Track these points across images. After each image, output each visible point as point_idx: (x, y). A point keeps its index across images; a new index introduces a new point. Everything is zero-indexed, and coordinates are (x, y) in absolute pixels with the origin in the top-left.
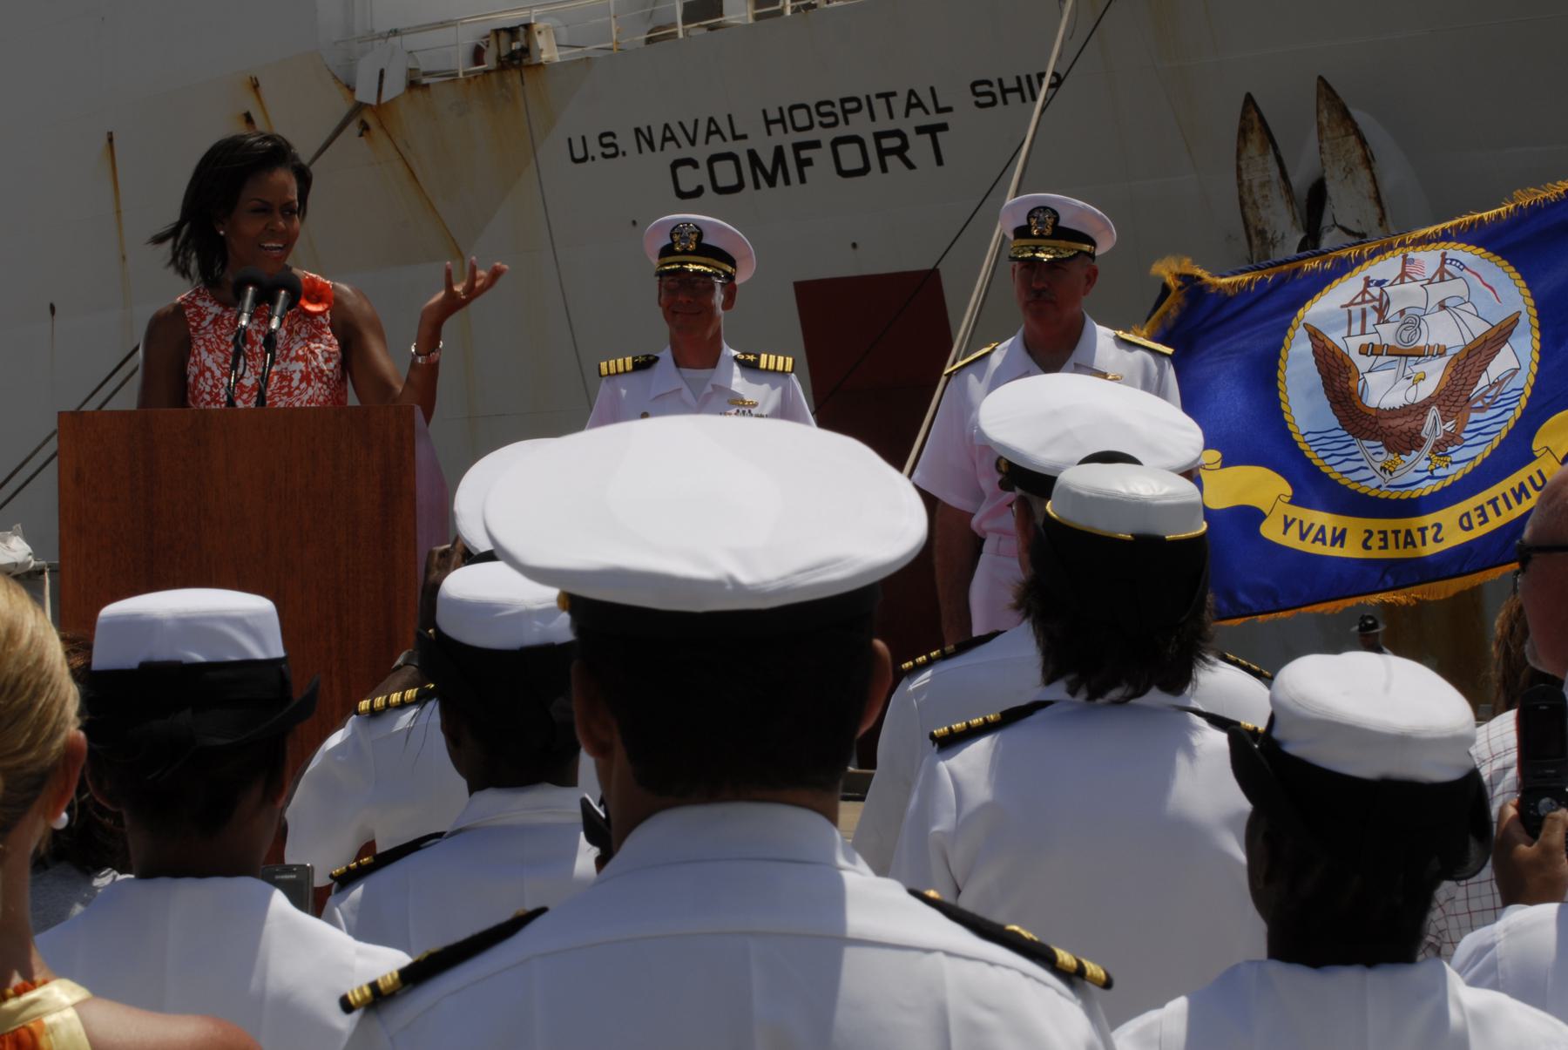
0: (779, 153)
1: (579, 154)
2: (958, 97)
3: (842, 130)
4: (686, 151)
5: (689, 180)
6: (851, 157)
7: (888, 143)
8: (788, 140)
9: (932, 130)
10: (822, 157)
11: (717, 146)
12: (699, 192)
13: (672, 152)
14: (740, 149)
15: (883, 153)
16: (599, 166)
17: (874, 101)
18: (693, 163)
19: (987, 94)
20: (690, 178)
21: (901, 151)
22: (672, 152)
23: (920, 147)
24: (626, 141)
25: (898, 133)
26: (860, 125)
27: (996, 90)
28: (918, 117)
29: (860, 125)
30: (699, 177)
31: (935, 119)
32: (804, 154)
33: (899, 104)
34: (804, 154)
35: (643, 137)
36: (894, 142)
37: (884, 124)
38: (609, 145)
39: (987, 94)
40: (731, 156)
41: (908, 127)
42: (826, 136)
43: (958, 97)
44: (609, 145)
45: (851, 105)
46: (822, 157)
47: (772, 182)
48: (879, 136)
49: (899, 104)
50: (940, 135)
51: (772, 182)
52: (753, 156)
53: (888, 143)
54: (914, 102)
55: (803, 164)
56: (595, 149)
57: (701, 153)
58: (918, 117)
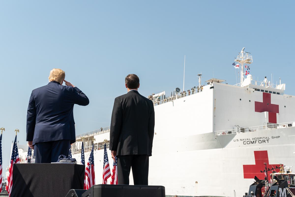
0: (253, 141)
1: (235, 141)
2: (270, 137)
3: (259, 140)
4: (245, 141)
5: (245, 143)
6: (260, 142)
7: (263, 141)
9: (268, 140)
10: (257, 142)
11: (248, 141)
13: (243, 141)
14: (250, 141)
15: (263, 142)
16: (236, 142)
17: (263, 138)
18: (245, 142)
19: (273, 137)
20: (245, 143)
22: (243, 141)
23: (266, 141)
24: (239, 140)
26: (261, 140)
27: (274, 137)
28: (267, 139)
31: (268, 139)
32: (256, 141)
33: (265, 138)
34: (256, 141)
35: (241, 140)
36: (264, 141)
37: (263, 139)
39: (273, 137)
41: (265, 139)
42: (258, 140)
43: (270, 137)
45: (261, 138)
46: (257, 142)
47: (253, 143)
48: (263, 140)
49: (265, 138)
50: (268, 140)
51: (253, 143)
52: (251, 142)
53: (263, 141)
54: (266, 138)
55: (255, 142)
56: (236, 140)
57: (246, 141)
58: (267, 139)
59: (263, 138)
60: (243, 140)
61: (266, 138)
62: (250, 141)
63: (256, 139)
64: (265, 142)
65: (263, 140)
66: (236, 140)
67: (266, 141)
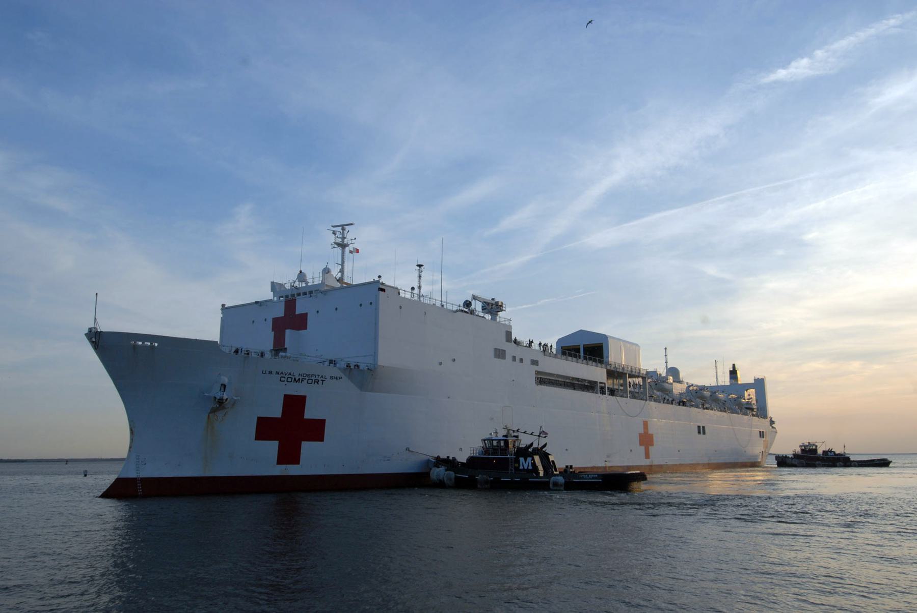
0: (299, 379)
4: (284, 376)
5: (283, 379)
6: (310, 381)
8: (301, 377)
9: (323, 381)
10: (306, 381)
11: (290, 376)
12: (284, 381)
13: (282, 375)
14: (293, 377)
15: (315, 382)
19: (332, 378)
20: (283, 379)
21: (317, 382)
22: (282, 375)
23: (320, 382)
24: (274, 372)
25: (318, 380)
28: (322, 379)
29: (313, 378)
30: (286, 379)
33: (320, 377)
38: (270, 373)
39: (332, 378)
40: (292, 378)
41: (319, 379)
43: (328, 377)
44: (270, 373)
47: (296, 382)
48: (315, 380)
49: (320, 377)
51: (296, 382)
52: (295, 379)
54: (322, 377)
55: (302, 381)
56: (267, 372)
57: (286, 377)
58: (322, 379)
59: (317, 376)
60: (282, 373)
61: (322, 377)
62: (293, 377)
63: (305, 375)
64: (317, 382)
65: (315, 380)
66: (267, 372)
67: (320, 381)
